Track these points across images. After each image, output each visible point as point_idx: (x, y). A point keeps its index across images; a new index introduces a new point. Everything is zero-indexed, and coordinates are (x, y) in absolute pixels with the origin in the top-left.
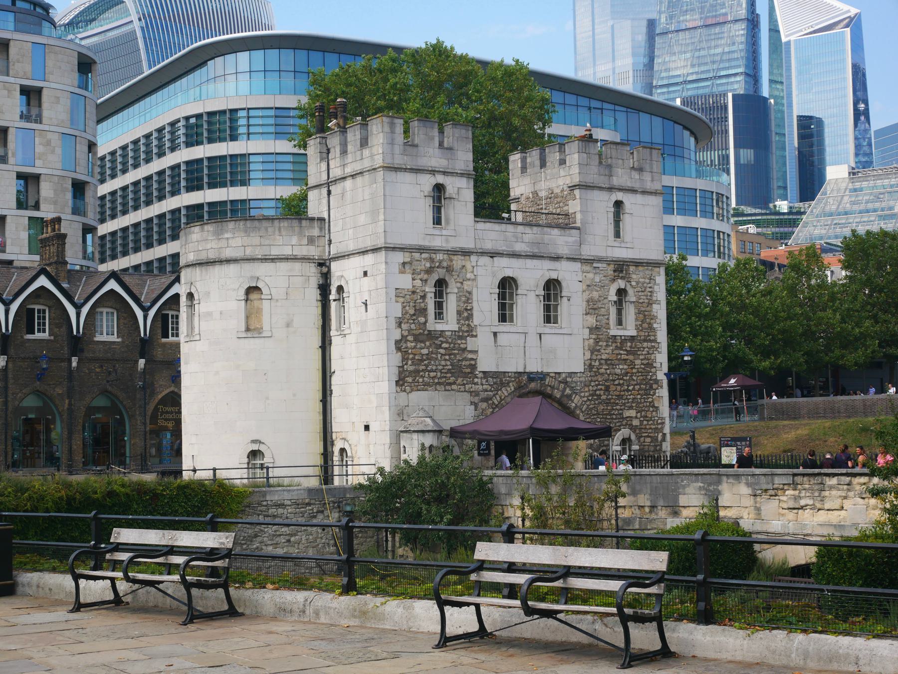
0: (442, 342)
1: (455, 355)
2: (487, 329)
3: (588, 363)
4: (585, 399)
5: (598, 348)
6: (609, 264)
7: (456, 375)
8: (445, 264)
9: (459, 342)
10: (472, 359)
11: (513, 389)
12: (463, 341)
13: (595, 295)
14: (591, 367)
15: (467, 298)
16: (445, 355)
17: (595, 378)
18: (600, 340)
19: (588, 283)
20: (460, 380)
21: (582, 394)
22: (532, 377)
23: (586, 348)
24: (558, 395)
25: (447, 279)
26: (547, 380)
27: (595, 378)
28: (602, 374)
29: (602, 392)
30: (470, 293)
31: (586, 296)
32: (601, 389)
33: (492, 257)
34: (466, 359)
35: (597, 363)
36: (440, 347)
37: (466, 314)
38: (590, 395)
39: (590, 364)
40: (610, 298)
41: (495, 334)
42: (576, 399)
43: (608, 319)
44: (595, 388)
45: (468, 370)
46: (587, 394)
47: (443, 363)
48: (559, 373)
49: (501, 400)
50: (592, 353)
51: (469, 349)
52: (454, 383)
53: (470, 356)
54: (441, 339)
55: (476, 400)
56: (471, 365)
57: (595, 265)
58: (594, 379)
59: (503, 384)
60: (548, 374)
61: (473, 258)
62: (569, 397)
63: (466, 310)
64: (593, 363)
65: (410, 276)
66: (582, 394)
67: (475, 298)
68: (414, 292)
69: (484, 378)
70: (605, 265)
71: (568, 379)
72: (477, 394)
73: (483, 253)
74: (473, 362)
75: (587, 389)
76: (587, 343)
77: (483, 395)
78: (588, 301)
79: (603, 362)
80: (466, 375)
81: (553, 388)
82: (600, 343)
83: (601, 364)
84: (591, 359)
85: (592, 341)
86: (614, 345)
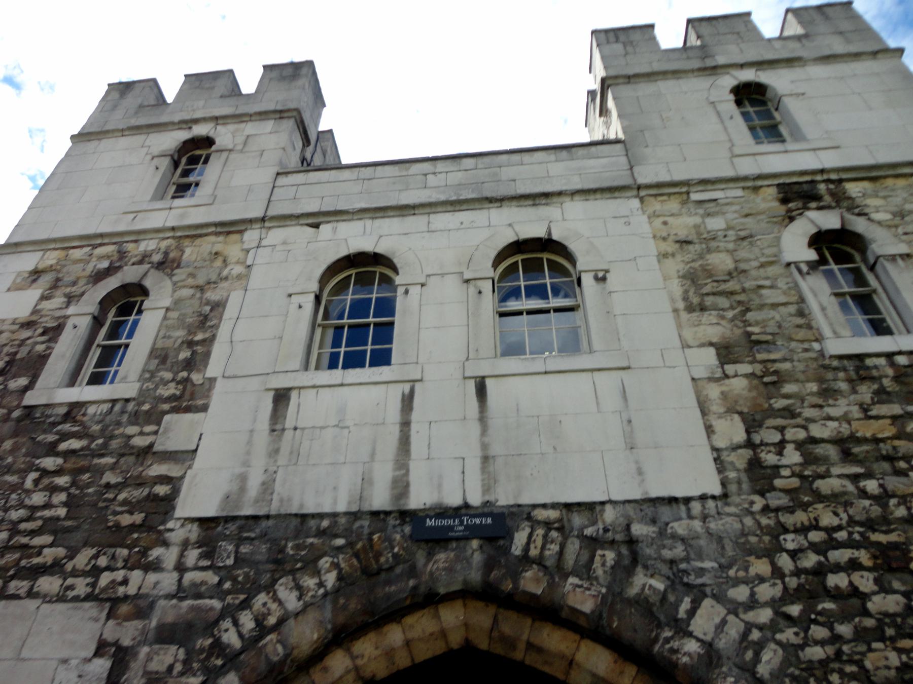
0: (65, 436)
1: (100, 471)
2: (255, 384)
3: (740, 459)
4: (765, 615)
5: (779, 403)
6: (756, 189)
7: (78, 537)
8: (157, 258)
9: (132, 430)
10: (164, 479)
11: (331, 579)
12: (149, 429)
13: (721, 261)
14: (760, 476)
15: (207, 319)
16: (59, 472)
17: (801, 517)
18: (780, 379)
19: (682, 237)
20: (82, 560)
21: (740, 593)
22: (432, 529)
23: (716, 407)
24: (582, 599)
25: (147, 283)
26: (520, 538)
27: (801, 517)
28: (836, 499)
29: (865, 582)
30: (219, 306)
31: (675, 266)
32: (854, 565)
33: (316, 226)
34: (140, 482)
35: (792, 456)
36: (51, 450)
37: (184, 354)
38: (788, 596)
39: (754, 464)
40: (788, 257)
41: (281, 397)
42: (706, 619)
43: (801, 313)
44: (810, 560)
45: (138, 518)
46: (766, 591)
47: (38, 498)
48: (590, 507)
49: (262, 629)
50: (752, 424)
51: (157, 448)
52: (55, 568)
53: (157, 470)
54: (67, 427)
55: (126, 633)
56: (153, 498)
57: (695, 197)
58: (788, 520)
59: (280, 565)
60: (522, 513)
61: (251, 236)
62: (657, 613)
63: (190, 344)
64: (770, 458)
65: (33, 295)
66: (740, 593)
67: (230, 312)
68: (28, 325)
69: (200, 544)
70: (739, 193)
71: (638, 529)
72: (141, 607)
73: (285, 219)
74: (162, 490)
75: (761, 567)
76: (713, 392)
77: (167, 612)
78: (691, 278)
79: (832, 451)
80: (118, 536)
81: (557, 571)
82: (789, 388)
83: (810, 459)
84: (749, 444)
85: (738, 385)
86: (866, 392)
